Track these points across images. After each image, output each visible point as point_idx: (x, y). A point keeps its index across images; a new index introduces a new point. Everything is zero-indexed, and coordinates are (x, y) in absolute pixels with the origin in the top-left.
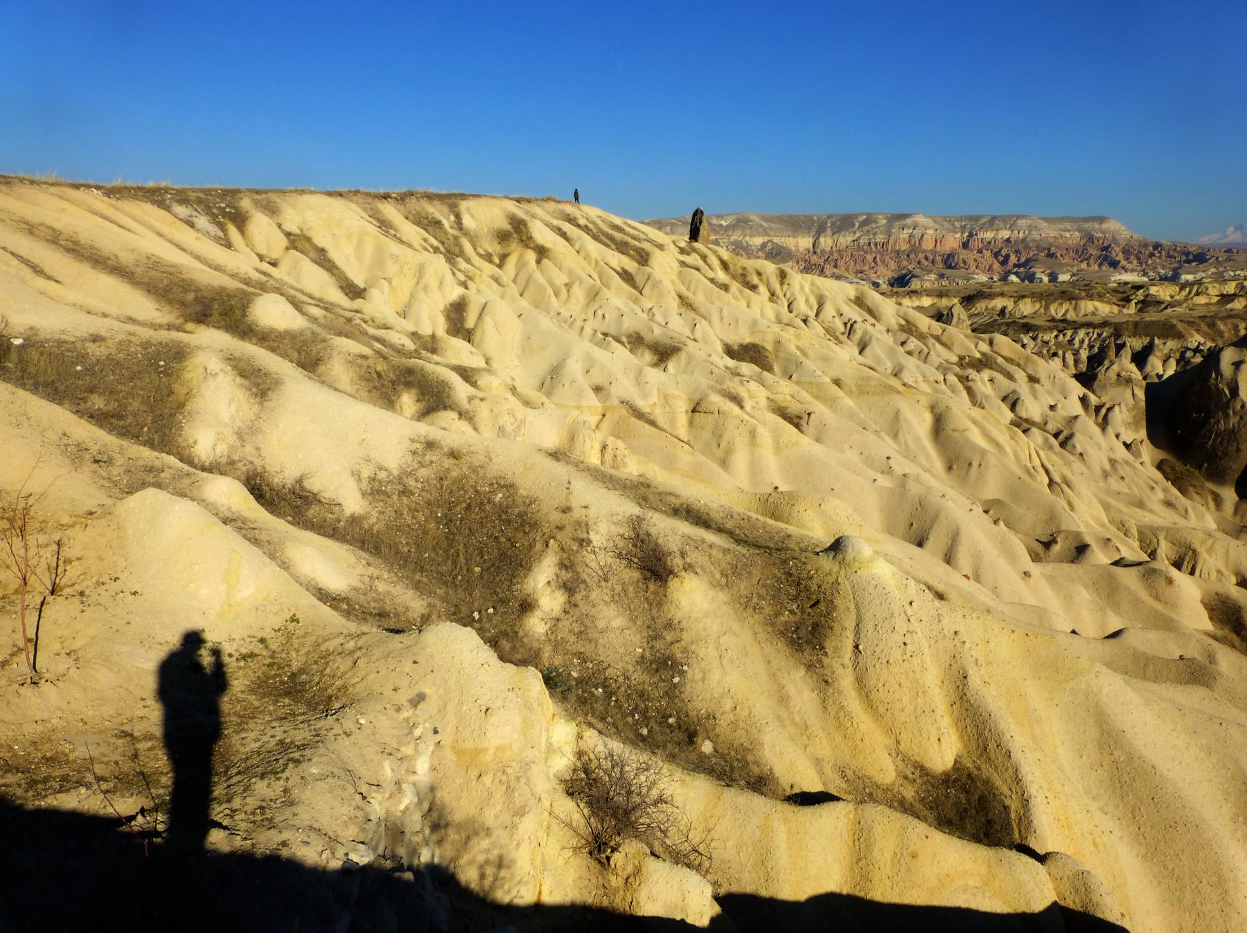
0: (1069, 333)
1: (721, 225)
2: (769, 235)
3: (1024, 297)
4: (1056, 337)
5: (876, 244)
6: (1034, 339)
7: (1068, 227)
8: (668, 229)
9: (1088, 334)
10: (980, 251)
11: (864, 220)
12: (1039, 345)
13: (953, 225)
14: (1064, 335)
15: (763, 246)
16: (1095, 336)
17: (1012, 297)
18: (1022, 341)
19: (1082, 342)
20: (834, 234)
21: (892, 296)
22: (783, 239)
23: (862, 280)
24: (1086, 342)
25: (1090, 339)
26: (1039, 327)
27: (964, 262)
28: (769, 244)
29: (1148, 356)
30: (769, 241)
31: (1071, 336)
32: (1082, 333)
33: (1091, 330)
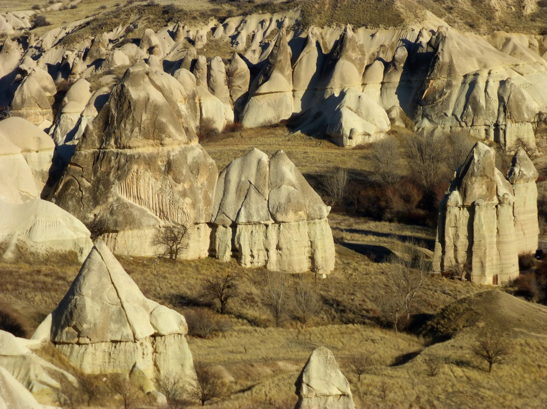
0: (233, 22)
4: (214, 30)
6: (174, 35)
9: (262, 23)
12: (181, 46)
14: (225, 26)
16: (274, 25)
18: (149, 41)
19: (252, 38)
24: (259, 38)
25: (265, 33)
26: (186, 14)
29: (336, 61)
31: (237, 29)
32: (253, 21)
33: (267, 16)
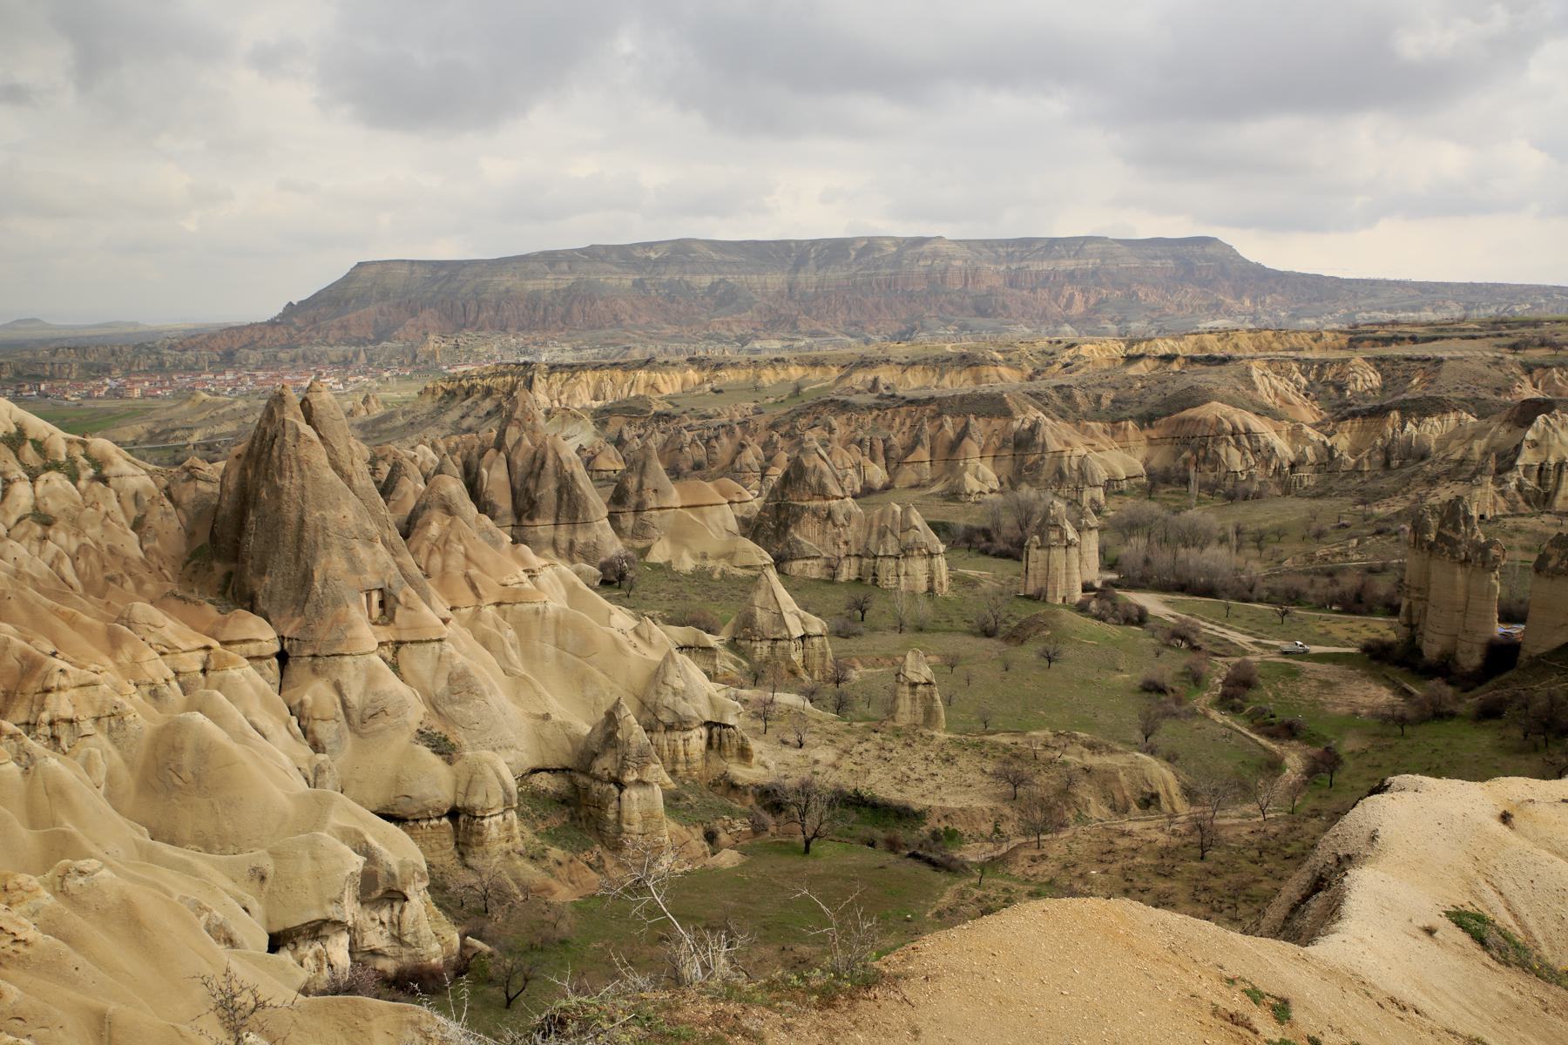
1: (648, 258)
2: (721, 273)
3: (914, 364)
5: (878, 284)
7: (1159, 253)
8: (565, 266)
10: (1033, 290)
11: (864, 247)
13: (996, 252)
15: (713, 287)
17: (900, 364)
20: (818, 268)
21: (748, 367)
22: (743, 277)
23: (852, 336)
27: (1005, 307)
28: (721, 286)
30: (721, 281)
